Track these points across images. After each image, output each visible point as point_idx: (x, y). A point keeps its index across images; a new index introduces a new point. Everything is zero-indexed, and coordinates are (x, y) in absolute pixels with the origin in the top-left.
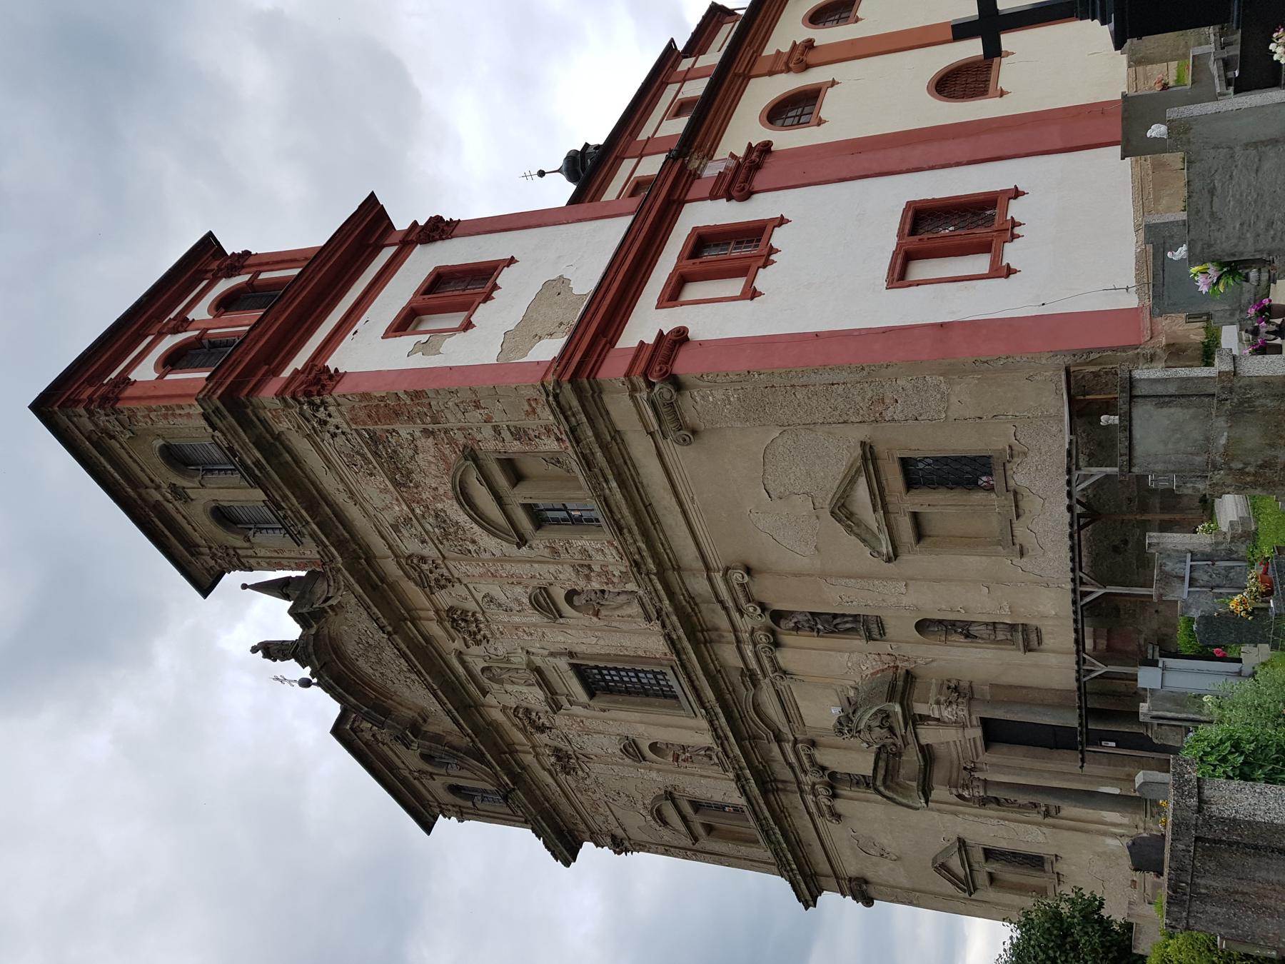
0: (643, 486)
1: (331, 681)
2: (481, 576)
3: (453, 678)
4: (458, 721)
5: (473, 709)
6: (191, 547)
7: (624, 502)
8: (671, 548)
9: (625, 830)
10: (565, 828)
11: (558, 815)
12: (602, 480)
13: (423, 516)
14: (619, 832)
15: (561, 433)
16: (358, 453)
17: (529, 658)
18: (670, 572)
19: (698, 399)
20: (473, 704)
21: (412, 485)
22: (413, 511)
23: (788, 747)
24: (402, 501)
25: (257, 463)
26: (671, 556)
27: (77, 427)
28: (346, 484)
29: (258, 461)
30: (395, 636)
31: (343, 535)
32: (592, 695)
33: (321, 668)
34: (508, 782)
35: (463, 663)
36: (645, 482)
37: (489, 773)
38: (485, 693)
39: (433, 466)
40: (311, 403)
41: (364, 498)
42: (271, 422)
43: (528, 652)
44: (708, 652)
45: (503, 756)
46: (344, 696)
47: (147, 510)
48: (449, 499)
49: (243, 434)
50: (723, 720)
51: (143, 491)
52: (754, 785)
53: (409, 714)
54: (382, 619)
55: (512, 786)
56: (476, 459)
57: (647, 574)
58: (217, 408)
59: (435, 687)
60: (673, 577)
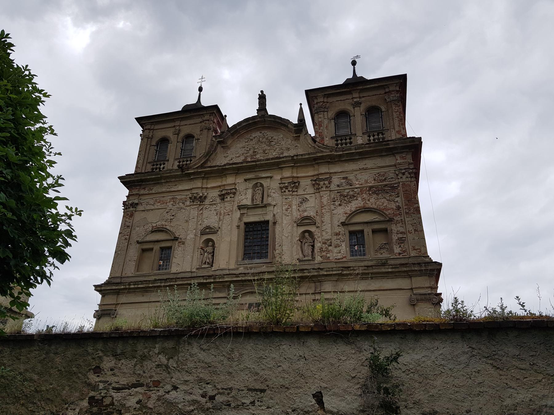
0: (382, 278)
1: (256, 120)
2: (322, 202)
4: (235, 165)
6: (328, 96)
7: (380, 271)
8: (348, 280)
9: (143, 211)
10: (144, 183)
11: (154, 183)
12: (393, 267)
13: (353, 191)
14: (140, 208)
15: (403, 256)
16: (385, 179)
17: (272, 206)
18: (337, 278)
19: (430, 309)
21: (371, 193)
22: (356, 188)
24: (361, 186)
25: (388, 145)
26: (344, 280)
28: (368, 169)
29: (389, 145)
30: (290, 158)
31: (343, 158)
34: (188, 172)
36: (383, 280)
39: (381, 204)
40: (412, 173)
42: (401, 155)
43: (275, 206)
45: (204, 174)
46: (247, 122)
47: (350, 89)
48: (364, 203)
51: (359, 91)
52: (202, 281)
53: (229, 142)
54: (301, 157)
55: (186, 172)
56: (388, 221)
57: (342, 270)
59: (257, 163)
60: (335, 278)
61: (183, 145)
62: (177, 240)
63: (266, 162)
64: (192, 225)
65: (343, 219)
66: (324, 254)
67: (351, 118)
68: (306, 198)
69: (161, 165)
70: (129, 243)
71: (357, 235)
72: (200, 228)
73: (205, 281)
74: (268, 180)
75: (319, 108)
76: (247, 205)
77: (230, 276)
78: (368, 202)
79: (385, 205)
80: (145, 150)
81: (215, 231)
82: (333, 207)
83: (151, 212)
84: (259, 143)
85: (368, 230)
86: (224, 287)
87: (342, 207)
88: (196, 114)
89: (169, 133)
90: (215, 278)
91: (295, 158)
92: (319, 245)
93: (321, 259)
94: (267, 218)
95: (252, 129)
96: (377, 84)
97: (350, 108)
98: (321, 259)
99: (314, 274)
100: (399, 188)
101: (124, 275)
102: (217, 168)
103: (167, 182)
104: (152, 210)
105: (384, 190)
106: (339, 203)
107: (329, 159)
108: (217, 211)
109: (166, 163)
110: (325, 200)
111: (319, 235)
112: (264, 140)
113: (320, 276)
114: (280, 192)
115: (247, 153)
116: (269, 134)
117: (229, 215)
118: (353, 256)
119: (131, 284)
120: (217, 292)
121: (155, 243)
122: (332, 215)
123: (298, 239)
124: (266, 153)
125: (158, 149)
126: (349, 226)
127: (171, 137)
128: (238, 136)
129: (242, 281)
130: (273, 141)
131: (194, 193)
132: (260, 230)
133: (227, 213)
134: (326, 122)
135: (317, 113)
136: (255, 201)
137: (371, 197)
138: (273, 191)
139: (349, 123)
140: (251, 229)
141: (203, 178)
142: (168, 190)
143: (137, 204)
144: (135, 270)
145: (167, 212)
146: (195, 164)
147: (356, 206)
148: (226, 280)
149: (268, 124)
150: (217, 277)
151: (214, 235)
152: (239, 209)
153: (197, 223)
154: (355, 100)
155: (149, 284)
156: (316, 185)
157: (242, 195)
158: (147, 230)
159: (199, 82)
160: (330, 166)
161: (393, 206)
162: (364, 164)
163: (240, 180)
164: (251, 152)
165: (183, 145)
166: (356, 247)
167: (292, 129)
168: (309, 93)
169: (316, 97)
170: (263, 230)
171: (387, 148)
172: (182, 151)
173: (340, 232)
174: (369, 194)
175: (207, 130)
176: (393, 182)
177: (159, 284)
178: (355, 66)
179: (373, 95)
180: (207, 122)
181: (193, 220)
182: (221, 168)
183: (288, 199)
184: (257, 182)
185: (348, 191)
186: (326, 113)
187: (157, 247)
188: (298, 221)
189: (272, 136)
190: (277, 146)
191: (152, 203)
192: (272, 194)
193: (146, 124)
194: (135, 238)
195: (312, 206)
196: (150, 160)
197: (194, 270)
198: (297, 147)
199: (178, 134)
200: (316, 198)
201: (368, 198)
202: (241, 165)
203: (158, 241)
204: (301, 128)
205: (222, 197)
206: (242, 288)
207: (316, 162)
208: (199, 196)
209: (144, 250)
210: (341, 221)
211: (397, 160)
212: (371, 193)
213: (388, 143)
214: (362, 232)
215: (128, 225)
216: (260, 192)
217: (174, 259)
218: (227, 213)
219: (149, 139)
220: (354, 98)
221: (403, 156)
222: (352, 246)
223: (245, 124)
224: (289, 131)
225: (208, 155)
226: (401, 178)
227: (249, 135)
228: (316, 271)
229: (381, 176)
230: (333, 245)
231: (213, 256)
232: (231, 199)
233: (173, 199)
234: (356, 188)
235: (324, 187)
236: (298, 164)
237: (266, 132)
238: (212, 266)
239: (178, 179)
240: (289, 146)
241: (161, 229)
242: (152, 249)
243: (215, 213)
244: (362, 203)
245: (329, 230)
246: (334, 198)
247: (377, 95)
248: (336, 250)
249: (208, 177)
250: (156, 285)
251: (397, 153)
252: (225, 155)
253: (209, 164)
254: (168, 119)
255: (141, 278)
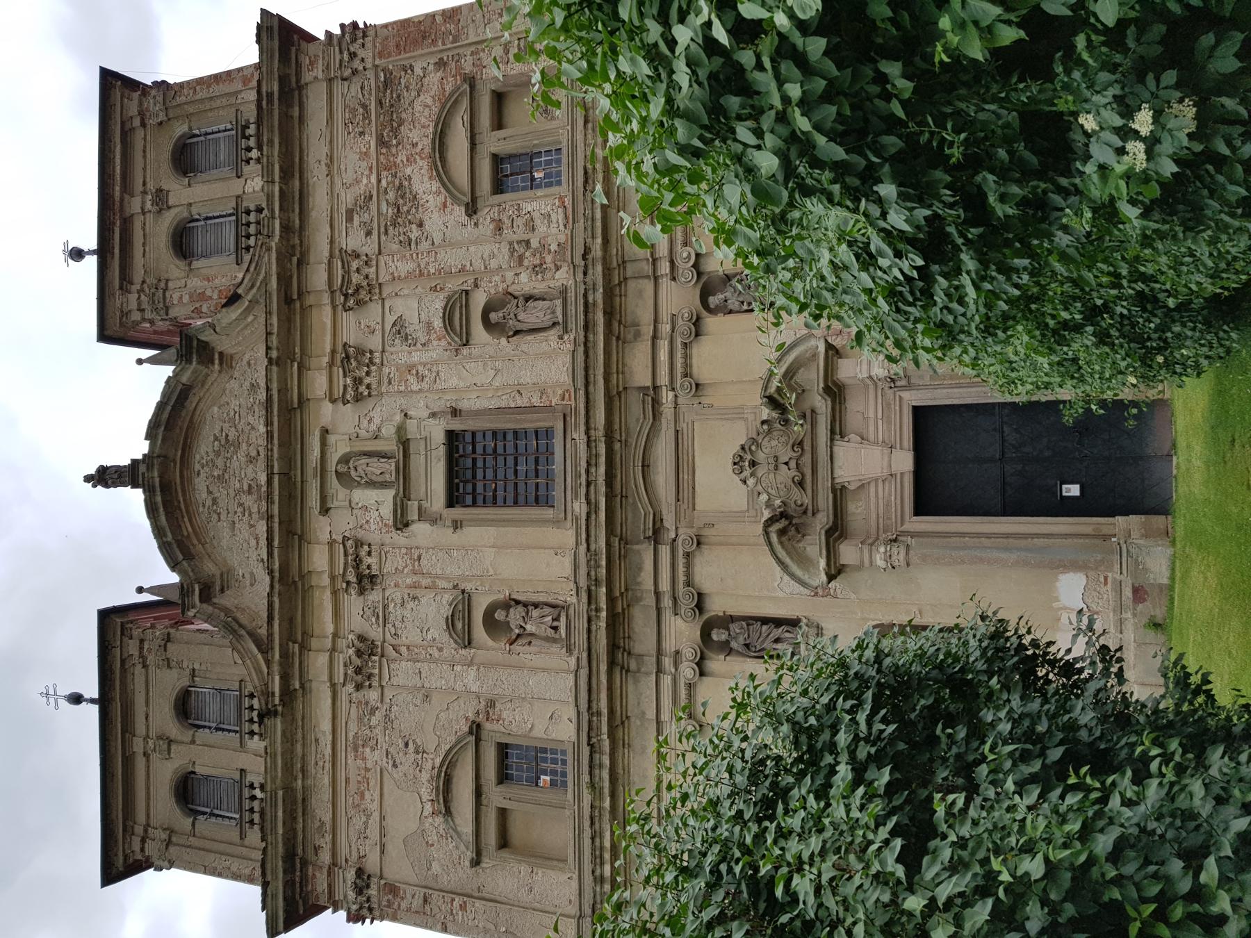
1: (157, 480)
2: (409, 277)
3: (299, 479)
4: (272, 540)
5: (296, 537)
6: (126, 278)
9: (382, 852)
10: (300, 851)
11: (303, 814)
14: (372, 864)
16: (364, 106)
20: (299, 532)
22: (379, 181)
23: (665, 551)
24: (374, 171)
25: (270, 95)
26: (621, 194)
27: (122, 106)
28: (332, 150)
29: (272, 94)
30: (275, 368)
31: (294, 222)
32: (453, 500)
33: (158, 456)
34: (277, 694)
35: (324, 444)
37: (261, 672)
38: (325, 510)
39: (427, 110)
41: (339, 169)
42: (304, 69)
43: (406, 415)
44: (618, 353)
45: (290, 644)
48: (422, 159)
49: (276, 61)
50: (602, 469)
51: (126, 197)
52: (603, 624)
53: (209, 568)
54: (274, 337)
55: (277, 701)
56: (472, 87)
58: (272, 27)
59: (276, 470)
61: (204, 727)
62: (479, 726)
63: (276, 441)
64: (438, 677)
65: (459, 212)
66: (549, 259)
67: (194, 211)
68: (394, 324)
69: (253, 798)
70: (476, 894)
71: (507, 176)
72: (450, 648)
73: (604, 614)
74: (332, 439)
75: (154, 302)
76: (395, 497)
77: (593, 533)
78: (420, 147)
79: (429, 101)
80: (202, 853)
81: (464, 598)
82: (425, 245)
83: (389, 822)
84: (227, 476)
85: (493, 143)
86: (625, 557)
87: (425, 218)
88: (118, 683)
89: (165, 772)
90: (596, 580)
91: (274, 354)
92: (524, 277)
93: (565, 269)
94: (439, 437)
95: (185, 500)
96: (115, 147)
97: (168, 220)
98: (565, 269)
99: (601, 273)
100: (391, 67)
101: (573, 910)
102: (276, 600)
103: (303, 771)
104: (382, 818)
105: (392, 106)
106: (414, 226)
107: (291, 260)
108: (406, 596)
109: (250, 778)
110: (403, 267)
111: (497, 278)
112: (220, 462)
113: (605, 260)
114: (370, 403)
115: (250, 515)
116: (204, 448)
117: (419, 558)
118: (559, 183)
119: (598, 872)
120: (639, 580)
121: (484, 802)
122: (446, 243)
123: (503, 341)
124: (258, 452)
125: (208, 810)
126: (478, 194)
127: (177, 765)
128: (195, 542)
129: (610, 497)
130: (227, 435)
131: (346, 674)
132: (474, 460)
133: (413, 566)
134: (195, 283)
135: (167, 308)
136: (387, 477)
137: (405, 140)
138: (365, 423)
139: (209, 222)
140: (469, 488)
141: (304, 647)
142: (328, 766)
143: (360, 872)
144: (560, 869)
145: (395, 766)
146: (258, 671)
147: (426, 179)
148: (603, 543)
149: (176, 450)
150: (593, 573)
151: (474, 603)
152: (407, 525)
153: (436, 661)
154: (148, 205)
155: (601, 808)
156: (361, 296)
157: (367, 522)
158: (442, 831)
159: (56, 704)
160: (312, 259)
161: (434, 78)
162: (316, 165)
163: (322, 529)
164: (249, 500)
165: (204, 727)
166: (538, 175)
167: (194, 372)
168: (108, 333)
169: (125, 314)
170: (474, 451)
171: (279, 99)
172: (223, 730)
173: (493, 220)
174: (397, 146)
175: (169, 645)
176: (373, 85)
177: (605, 774)
178: (86, 250)
179: (145, 157)
180: (146, 647)
181: (423, 675)
182: (277, 586)
183: (392, 375)
184: (334, 473)
185: (384, 205)
186: (170, 284)
187: (496, 796)
188: (455, 342)
189: (212, 438)
190: (243, 421)
191: (364, 819)
192: (373, 427)
193: (128, 851)
194: (462, 875)
195: (416, 306)
196: (234, 835)
197: (573, 661)
198: (252, 362)
199: (170, 742)
200: (396, 294)
201: (408, 147)
202: (276, 520)
203: (478, 793)
204: (195, 343)
205: (366, 581)
206: (630, 500)
207: (295, 297)
208: (354, 657)
209: (504, 842)
210: (465, 218)
211: (316, 78)
212: (394, 142)
213: (264, 94)
214: (497, 160)
215: (421, 901)
216: (364, 461)
217: (536, 733)
218: (413, 566)
219: (174, 839)
220: (142, 209)
221: (308, 62)
222: (533, 184)
223: (163, 518)
224: (203, 385)
225: (235, 631)
226: (363, 60)
227: (201, 509)
228: (590, 267)
229: (355, 116)
230: (526, 237)
231: (536, 606)
232: (373, 553)
233: (356, 749)
234: (379, 181)
235: (366, 270)
236: (297, 350)
237: (198, 457)
238: (565, 607)
239: (300, 731)
240: (247, 384)
241: (441, 783)
242: (503, 813)
243: (411, 605)
244: (420, 163)
245: (486, 250)
246: (401, 242)
247: (145, 147)
248: (542, 228)
249: (304, 633)
250: (606, 784)
251: (298, 74)
252: (248, 583)
253: (263, 632)
254: (120, 777)
255: (586, 845)
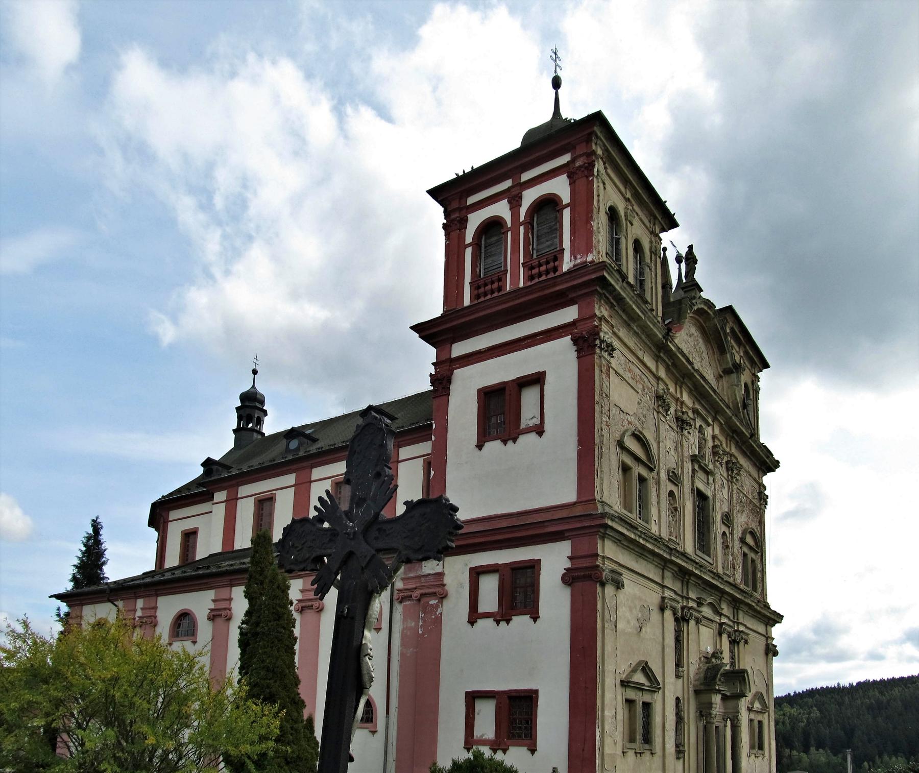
119: (643, 536)
167: (728, 362)
224: (718, 360)
